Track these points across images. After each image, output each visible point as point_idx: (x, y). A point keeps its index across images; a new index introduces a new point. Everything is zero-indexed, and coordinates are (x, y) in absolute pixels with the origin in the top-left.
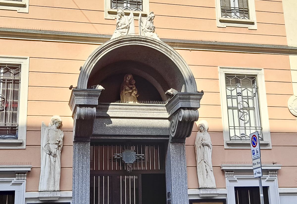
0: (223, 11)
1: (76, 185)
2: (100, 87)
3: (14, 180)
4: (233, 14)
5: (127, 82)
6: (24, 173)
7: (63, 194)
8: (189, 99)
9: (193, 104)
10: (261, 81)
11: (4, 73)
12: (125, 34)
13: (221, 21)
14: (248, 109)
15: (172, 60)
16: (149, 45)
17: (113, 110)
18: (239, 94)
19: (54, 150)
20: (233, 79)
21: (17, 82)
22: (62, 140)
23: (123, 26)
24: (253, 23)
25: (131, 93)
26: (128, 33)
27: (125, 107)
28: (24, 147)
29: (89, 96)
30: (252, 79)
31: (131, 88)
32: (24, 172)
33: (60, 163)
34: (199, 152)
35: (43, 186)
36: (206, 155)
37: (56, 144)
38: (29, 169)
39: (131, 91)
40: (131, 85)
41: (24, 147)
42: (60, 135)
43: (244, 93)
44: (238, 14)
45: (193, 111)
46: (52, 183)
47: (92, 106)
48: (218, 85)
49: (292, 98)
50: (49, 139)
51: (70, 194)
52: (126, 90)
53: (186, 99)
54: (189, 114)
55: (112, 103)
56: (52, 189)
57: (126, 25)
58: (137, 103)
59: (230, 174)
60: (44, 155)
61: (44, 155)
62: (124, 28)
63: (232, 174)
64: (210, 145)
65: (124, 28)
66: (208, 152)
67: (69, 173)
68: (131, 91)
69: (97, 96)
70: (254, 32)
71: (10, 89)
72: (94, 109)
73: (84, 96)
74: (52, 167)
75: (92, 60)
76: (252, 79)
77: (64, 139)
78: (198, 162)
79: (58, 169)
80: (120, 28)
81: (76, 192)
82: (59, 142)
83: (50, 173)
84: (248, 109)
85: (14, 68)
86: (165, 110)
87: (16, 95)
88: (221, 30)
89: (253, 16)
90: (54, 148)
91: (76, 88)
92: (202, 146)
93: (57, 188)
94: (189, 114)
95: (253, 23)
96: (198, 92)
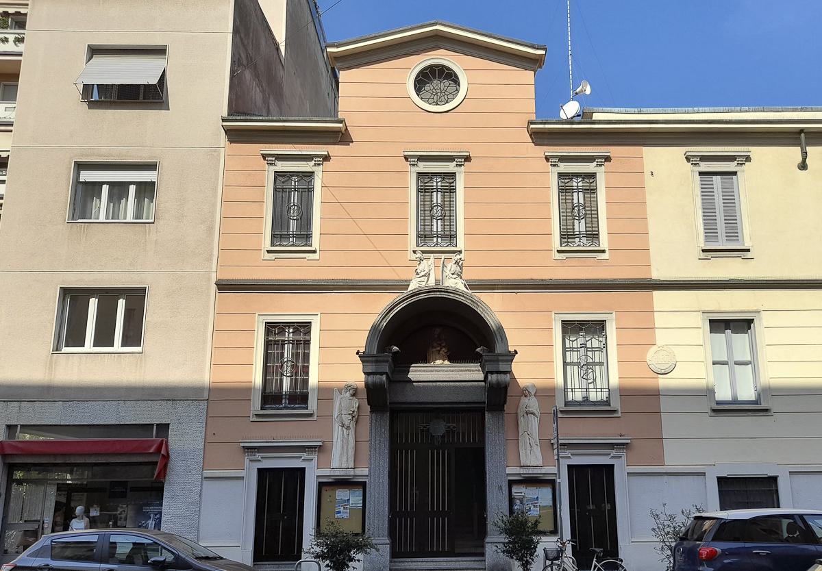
0: (562, 237)
1: (373, 462)
2: (395, 348)
3: (305, 455)
4: (577, 240)
5: (436, 336)
6: (315, 448)
7: (359, 472)
8: (498, 361)
9: (502, 367)
10: (611, 329)
11: (293, 332)
12: (424, 284)
13: (559, 252)
14: (594, 364)
15: (479, 312)
16: (451, 296)
17: (418, 373)
18: (584, 345)
19: (347, 422)
20: (571, 328)
21: (307, 343)
22: (356, 410)
23: (423, 273)
24: (604, 251)
25: (439, 351)
26: (429, 282)
27: (430, 369)
28: (315, 418)
29: (377, 361)
30: (598, 327)
31: (440, 345)
32: (315, 447)
33: (354, 436)
34: (522, 421)
35: (335, 463)
36: (532, 428)
37: (350, 414)
38: (320, 444)
39: (439, 348)
40: (440, 340)
41: (315, 418)
42: (355, 403)
43: (589, 345)
44: (584, 240)
45: (502, 375)
46: (344, 459)
47: (381, 374)
48: (551, 337)
49: (654, 349)
50: (342, 406)
51: (366, 472)
52: (433, 347)
53: (494, 361)
54: (497, 380)
55: (413, 365)
56: (344, 466)
57: (426, 272)
58: (447, 362)
59: (620, 448)
60: (337, 427)
61: (337, 427)
62: (423, 276)
63: (564, 449)
64: (537, 414)
65: (423, 276)
66: (534, 423)
67: (365, 447)
68: (439, 348)
69: (387, 361)
70: (604, 263)
71: (300, 351)
72: (384, 377)
73: (372, 362)
74: (344, 441)
75: (383, 319)
76: (598, 327)
77: (358, 408)
78: (520, 434)
79: (352, 443)
80: (421, 275)
81: (373, 470)
82: (353, 411)
83: (343, 448)
84: (594, 364)
85: (304, 327)
86: (479, 371)
87: (306, 357)
88: (559, 263)
89: (604, 242)
90: (347, 420)
91: (364, 353)
92: (525, 415)
93: (351, 465)
94: (497, 380)
95: (604, 251)
96: (510, 352)
